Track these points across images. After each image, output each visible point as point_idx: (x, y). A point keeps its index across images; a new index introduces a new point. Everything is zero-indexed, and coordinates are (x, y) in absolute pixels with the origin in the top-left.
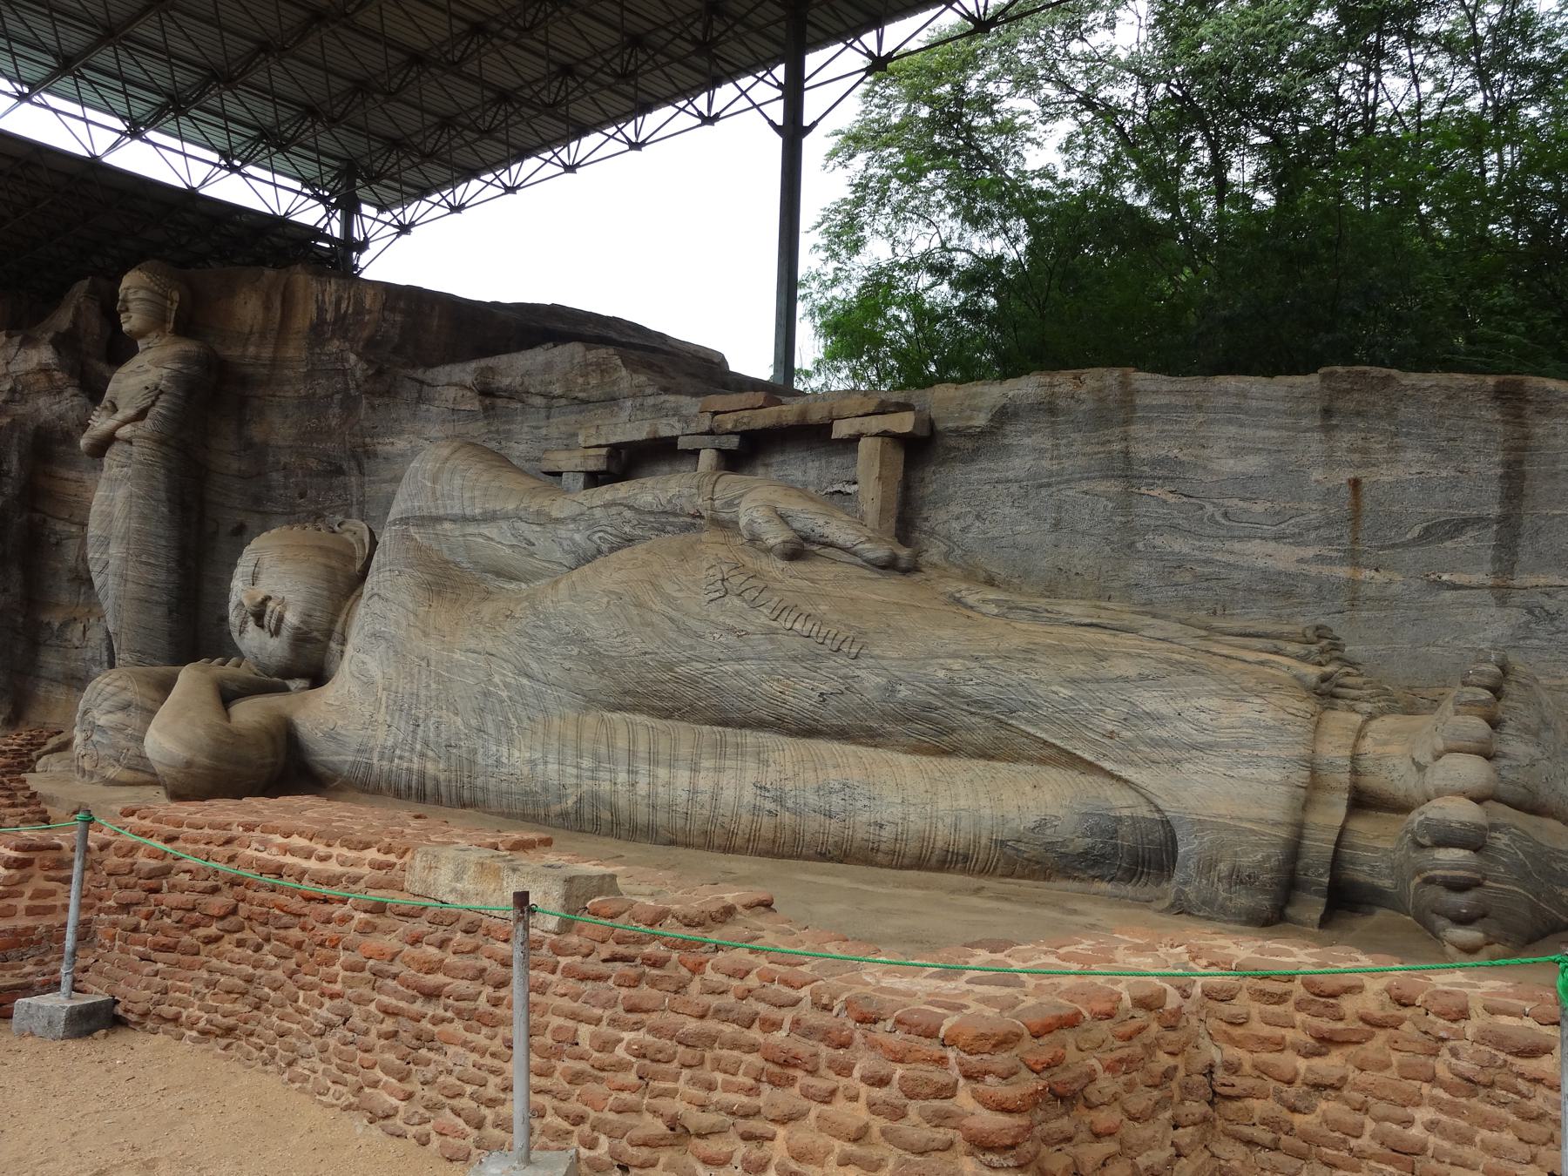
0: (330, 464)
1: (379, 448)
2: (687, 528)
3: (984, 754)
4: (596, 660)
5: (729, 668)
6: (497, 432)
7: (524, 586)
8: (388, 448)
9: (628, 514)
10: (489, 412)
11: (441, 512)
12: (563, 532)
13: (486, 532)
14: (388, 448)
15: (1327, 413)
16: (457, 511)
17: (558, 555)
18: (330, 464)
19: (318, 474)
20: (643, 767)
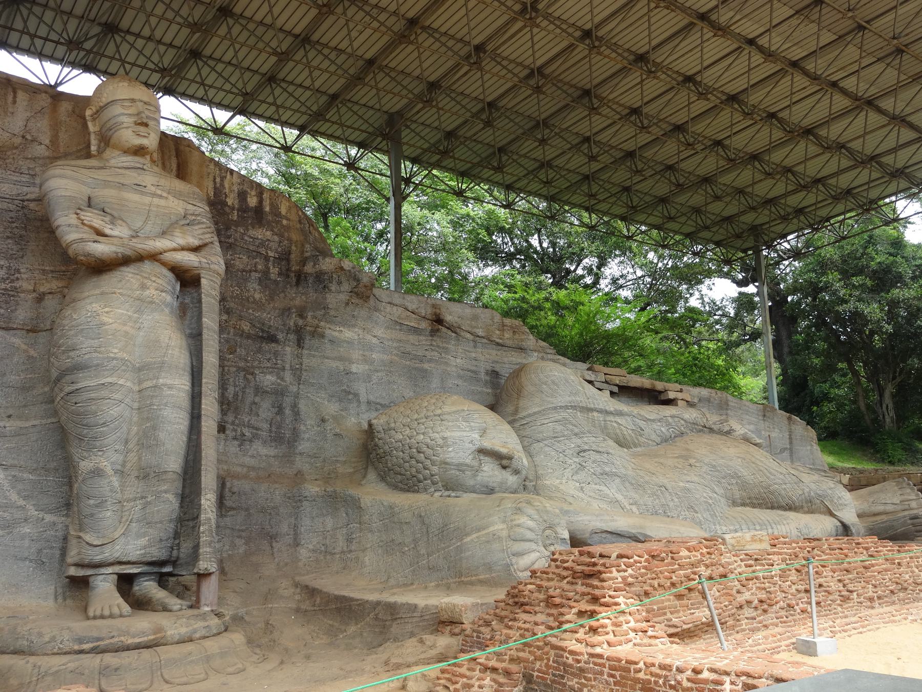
0: (263, 331)
1: (328, 332)
2: (700, 431)
3: (812, 513)
4: (744, 486)
5: (784, 486)
6: (438, 346)
7: (625, 450)
8: (336, 334)
9: (682, 422)
10: (434, 332)
11: (592, 406)
12: (656, 426)
13: (619, 421)
14: (336, 334)
15: (764, 416)
16: (601, 406)
17: (654, 437)
18: (263, 331)
19: (249, 337)
20: (774, 525)
